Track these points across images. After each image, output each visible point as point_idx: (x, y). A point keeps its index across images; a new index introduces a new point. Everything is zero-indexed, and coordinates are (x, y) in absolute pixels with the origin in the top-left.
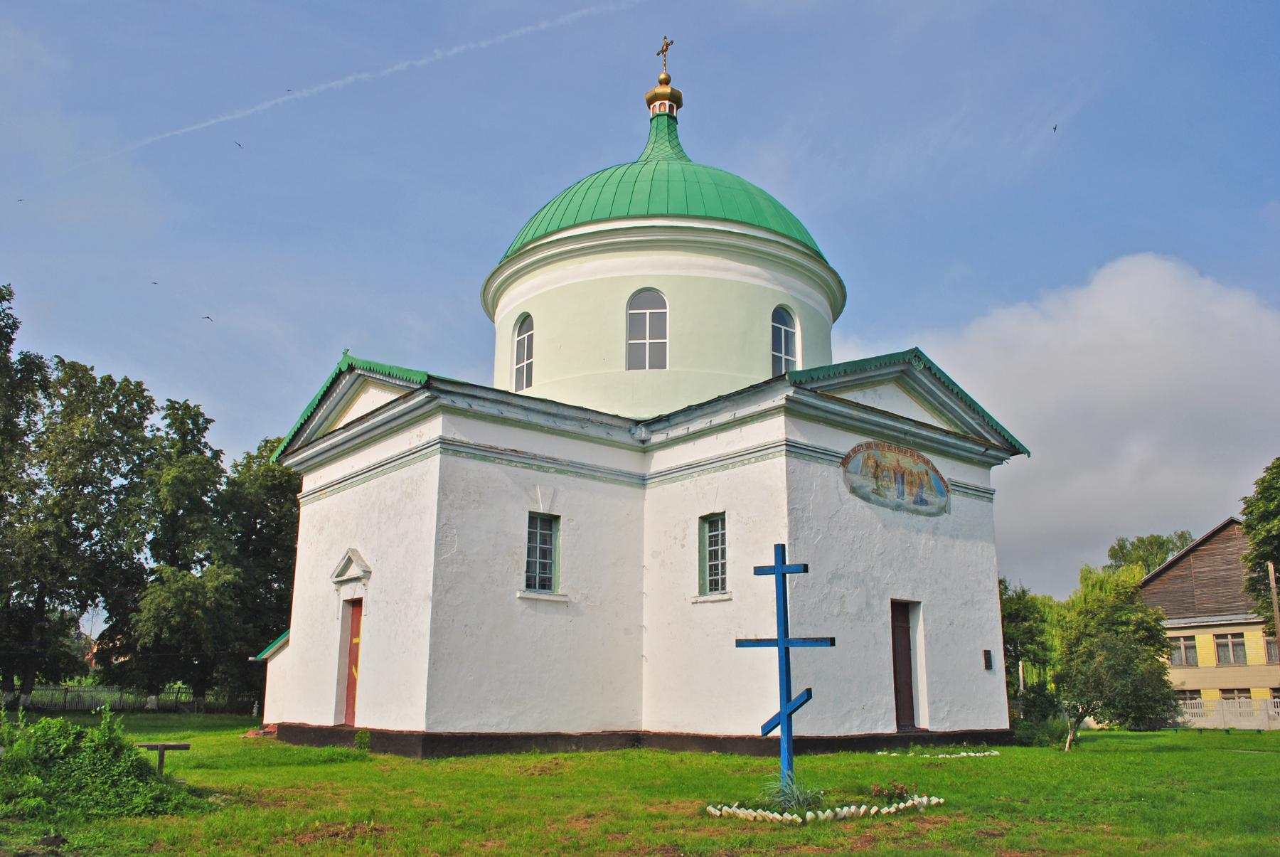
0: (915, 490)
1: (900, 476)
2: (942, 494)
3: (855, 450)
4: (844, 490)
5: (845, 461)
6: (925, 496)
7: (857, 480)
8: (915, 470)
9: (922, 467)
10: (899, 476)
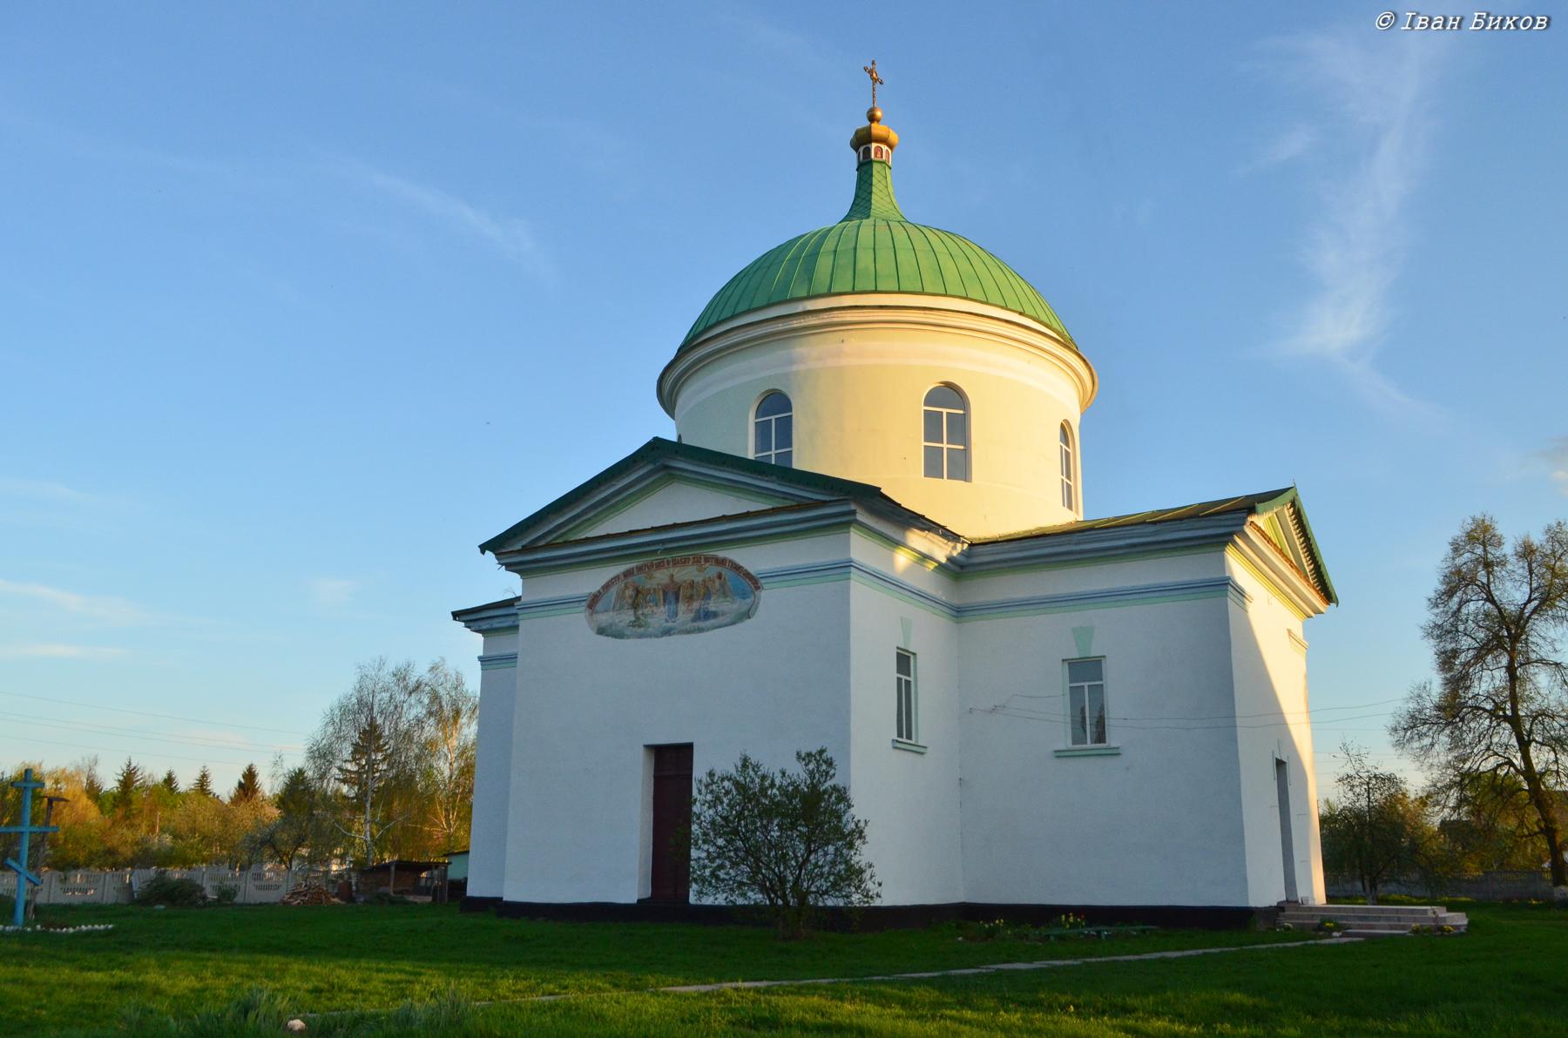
0: (696, 605)
1: (673, 593)
2: (744, 596)
3: (607, 587)
4: (591, 634)
5: (593, 602)
6: (712, 607)
7: (604, 618)
8: (699, 579)
9: (712, 570)
10: (671, 596)
